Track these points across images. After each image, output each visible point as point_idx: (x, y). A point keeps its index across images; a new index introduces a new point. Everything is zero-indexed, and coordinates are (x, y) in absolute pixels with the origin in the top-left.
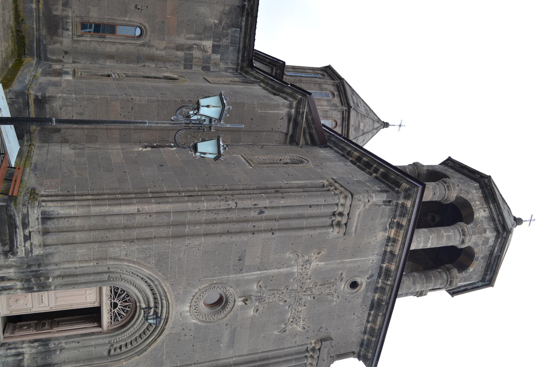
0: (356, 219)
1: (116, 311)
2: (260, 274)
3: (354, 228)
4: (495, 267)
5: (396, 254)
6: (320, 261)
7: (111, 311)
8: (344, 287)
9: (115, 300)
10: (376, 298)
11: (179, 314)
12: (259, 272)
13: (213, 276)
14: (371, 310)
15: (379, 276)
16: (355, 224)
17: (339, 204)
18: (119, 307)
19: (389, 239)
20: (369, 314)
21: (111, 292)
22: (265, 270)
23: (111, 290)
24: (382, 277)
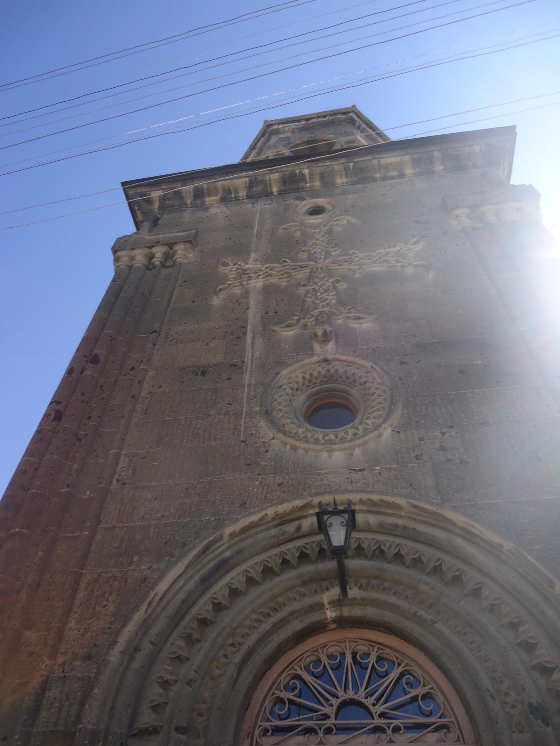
0: (161, 236)
1: (380, 708)
2: (254, 333)
3: (181, 234)
4: (325, 117)
5: (247, 180)
6: (248, 259)
7: (378, 729)
8: (315, 220)
9: (327, 710)
10: (345, 180)
11: (355, 476)
12: (249, 336)
13: (238, 415)
14: (374, 180)
15: (298, 190)
16: (173, 234)
17: (130, 264)
18: (360, 696)
19: (223, 200)
20: (385, 178)
21: (290, 729)
22: (244, 327)
23: (277, 730)
24: (301, 185)
